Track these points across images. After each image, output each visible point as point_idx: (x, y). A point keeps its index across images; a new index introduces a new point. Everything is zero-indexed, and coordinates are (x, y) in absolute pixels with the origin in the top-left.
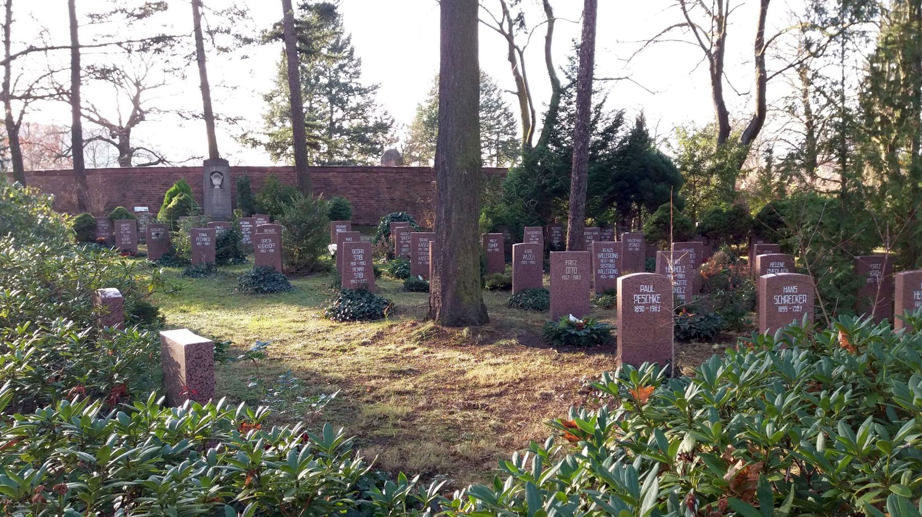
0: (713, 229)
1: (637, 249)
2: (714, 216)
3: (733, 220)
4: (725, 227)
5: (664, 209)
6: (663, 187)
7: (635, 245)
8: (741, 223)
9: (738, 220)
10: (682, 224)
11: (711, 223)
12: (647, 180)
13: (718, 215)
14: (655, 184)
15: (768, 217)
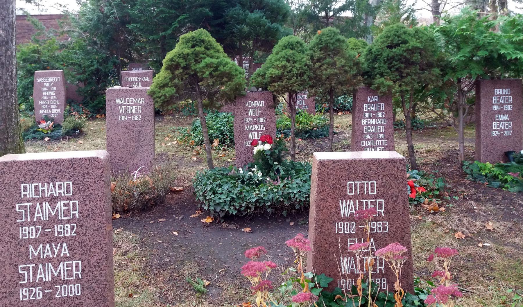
0: (280, 78)
1: (137, 118)
2: (282, 54)
3: (318, 60)
4: (301, 75)
5: (188, 41)
6: (258, 15)
7: (132, 110)
8: (333, 65)
9: (328, 60)
10: (216, 69)
11: (277, 67)
12: (238, 7)
13: (290, 52)
14: (248, 11)
15: (386, 53)
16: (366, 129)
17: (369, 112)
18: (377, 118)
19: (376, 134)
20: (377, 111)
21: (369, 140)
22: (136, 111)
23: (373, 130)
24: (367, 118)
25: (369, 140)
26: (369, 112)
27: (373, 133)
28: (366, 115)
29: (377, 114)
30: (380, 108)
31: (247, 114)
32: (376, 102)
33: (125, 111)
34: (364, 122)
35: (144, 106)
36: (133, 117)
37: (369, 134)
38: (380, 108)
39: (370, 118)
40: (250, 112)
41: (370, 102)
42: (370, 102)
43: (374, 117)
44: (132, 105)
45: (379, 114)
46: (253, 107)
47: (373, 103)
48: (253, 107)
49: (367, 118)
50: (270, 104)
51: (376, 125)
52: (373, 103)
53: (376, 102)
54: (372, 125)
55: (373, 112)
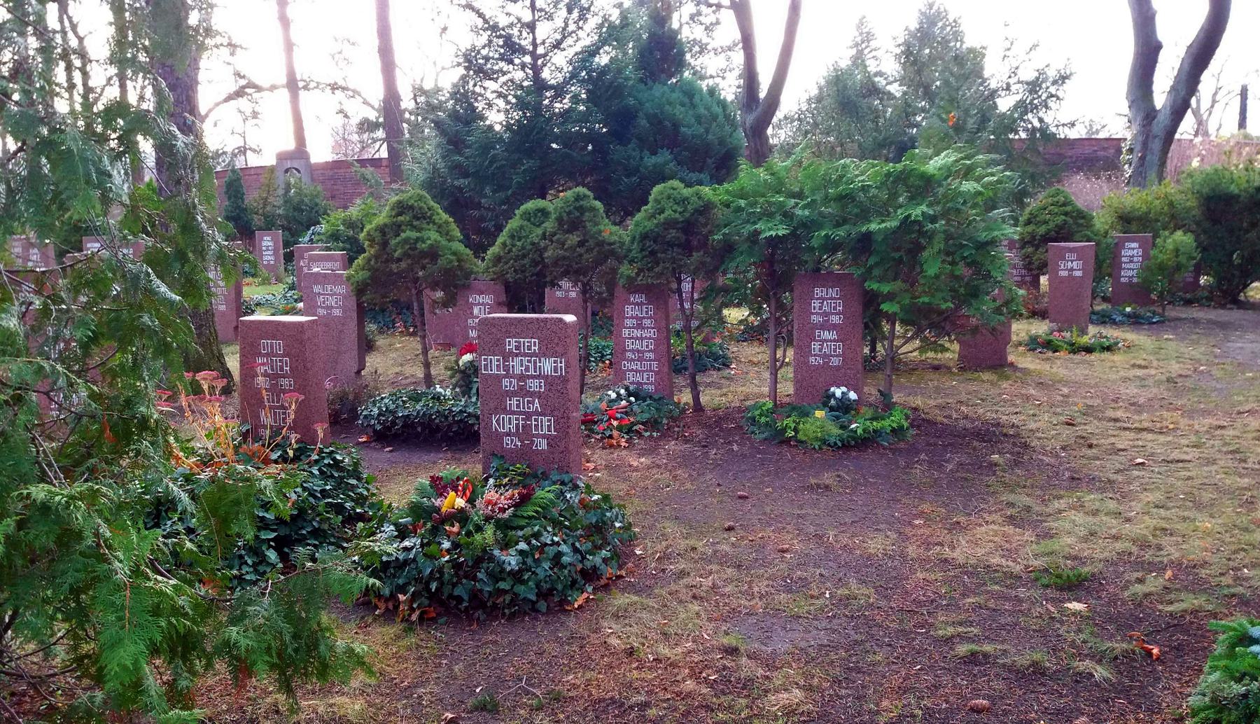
1: (337, 312)
7: (332, 301)
16: (629, 344)
17: (632, 317)
18: (644, 328)
19: (643, 352)
20: (644, 318)
21: (632, 360)
22: (336, 303)
23: (637, 346)
24: (630, 328)
25: (632, 360)
26: (632, 317)
27: (638, 351)
28: (628, 322)
29: (644, 321)
30: (647, 312)
31: (472, 313)
32: (641, 304)
33: (324, 302)
34: (626, 332)
35: (345, 297)
36: (333, 310)
37: (633, 351)
38: (647, 312)
39: (633, 328)
40: (476, 311)
41: (633, 304)
42: (633, 304)
43: (640, 326)
44: (332, 295)
45: (647, 322)
46: (479, 304)
47: (637, 304)
48: (479, 304)
49: (630, 328)
50: (501, 300)
51: (642, 339)
52: (637, 304)
53: (641, 304)
54: (637, 338)
55: (637, 318)
